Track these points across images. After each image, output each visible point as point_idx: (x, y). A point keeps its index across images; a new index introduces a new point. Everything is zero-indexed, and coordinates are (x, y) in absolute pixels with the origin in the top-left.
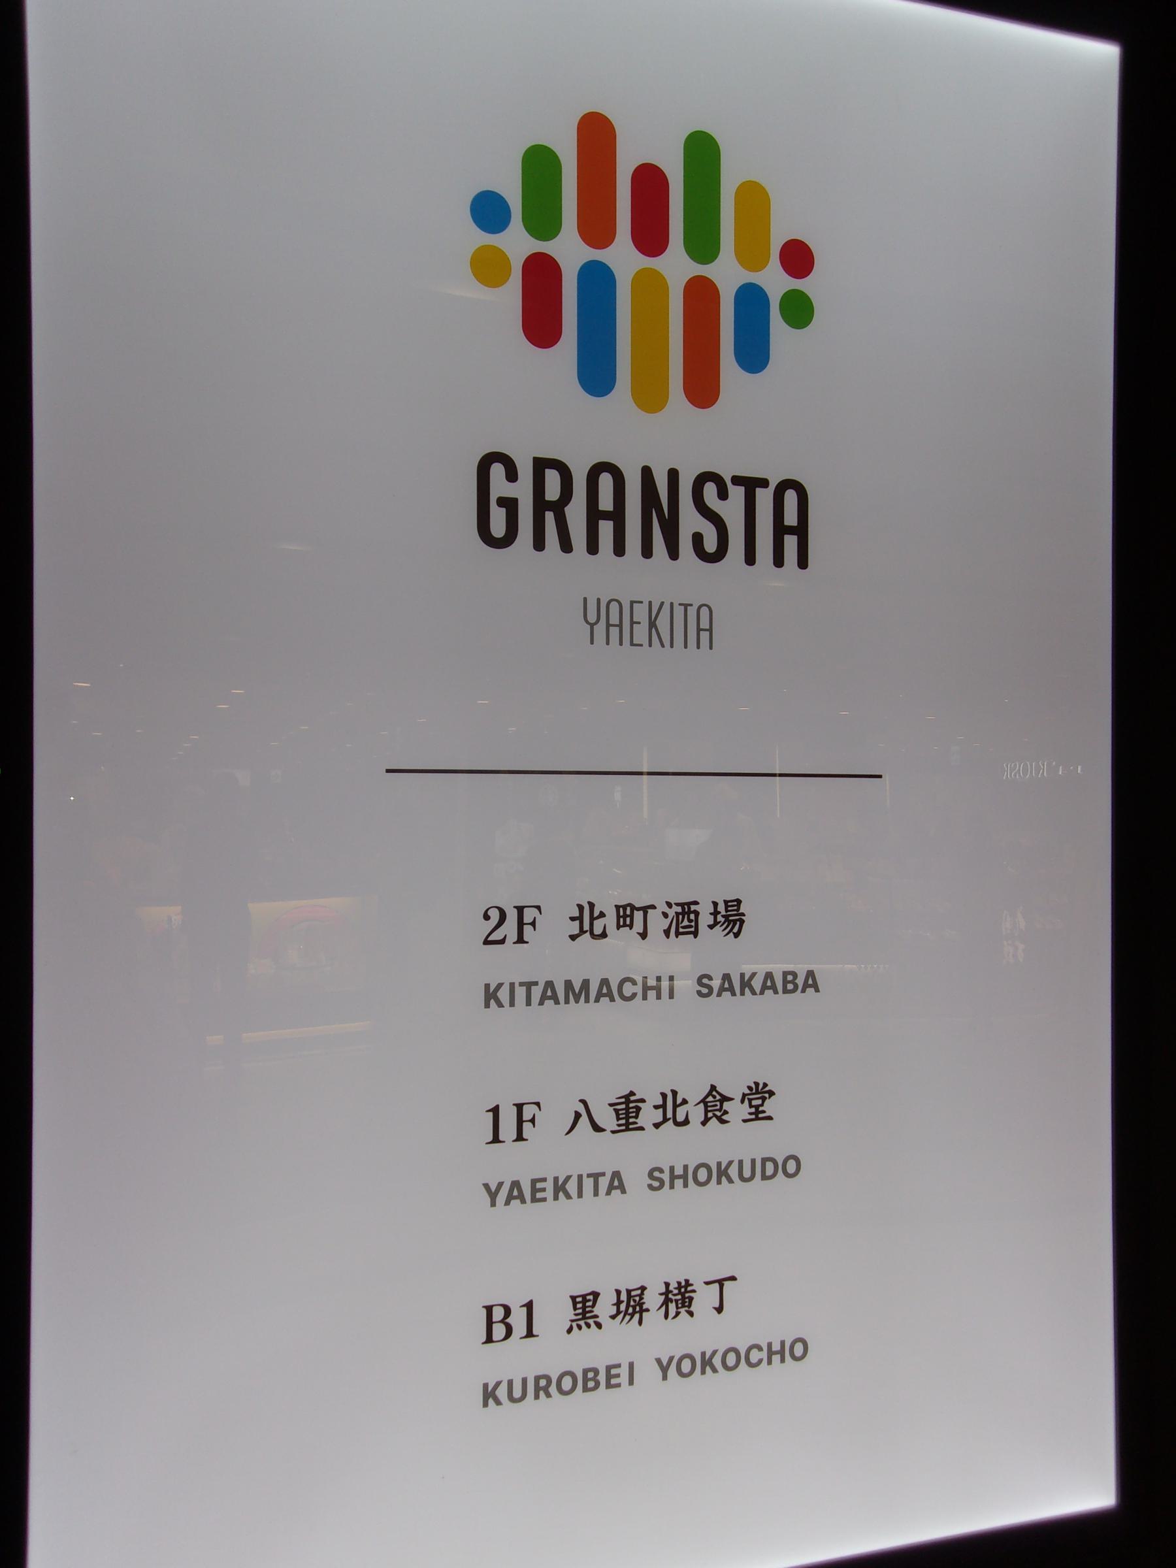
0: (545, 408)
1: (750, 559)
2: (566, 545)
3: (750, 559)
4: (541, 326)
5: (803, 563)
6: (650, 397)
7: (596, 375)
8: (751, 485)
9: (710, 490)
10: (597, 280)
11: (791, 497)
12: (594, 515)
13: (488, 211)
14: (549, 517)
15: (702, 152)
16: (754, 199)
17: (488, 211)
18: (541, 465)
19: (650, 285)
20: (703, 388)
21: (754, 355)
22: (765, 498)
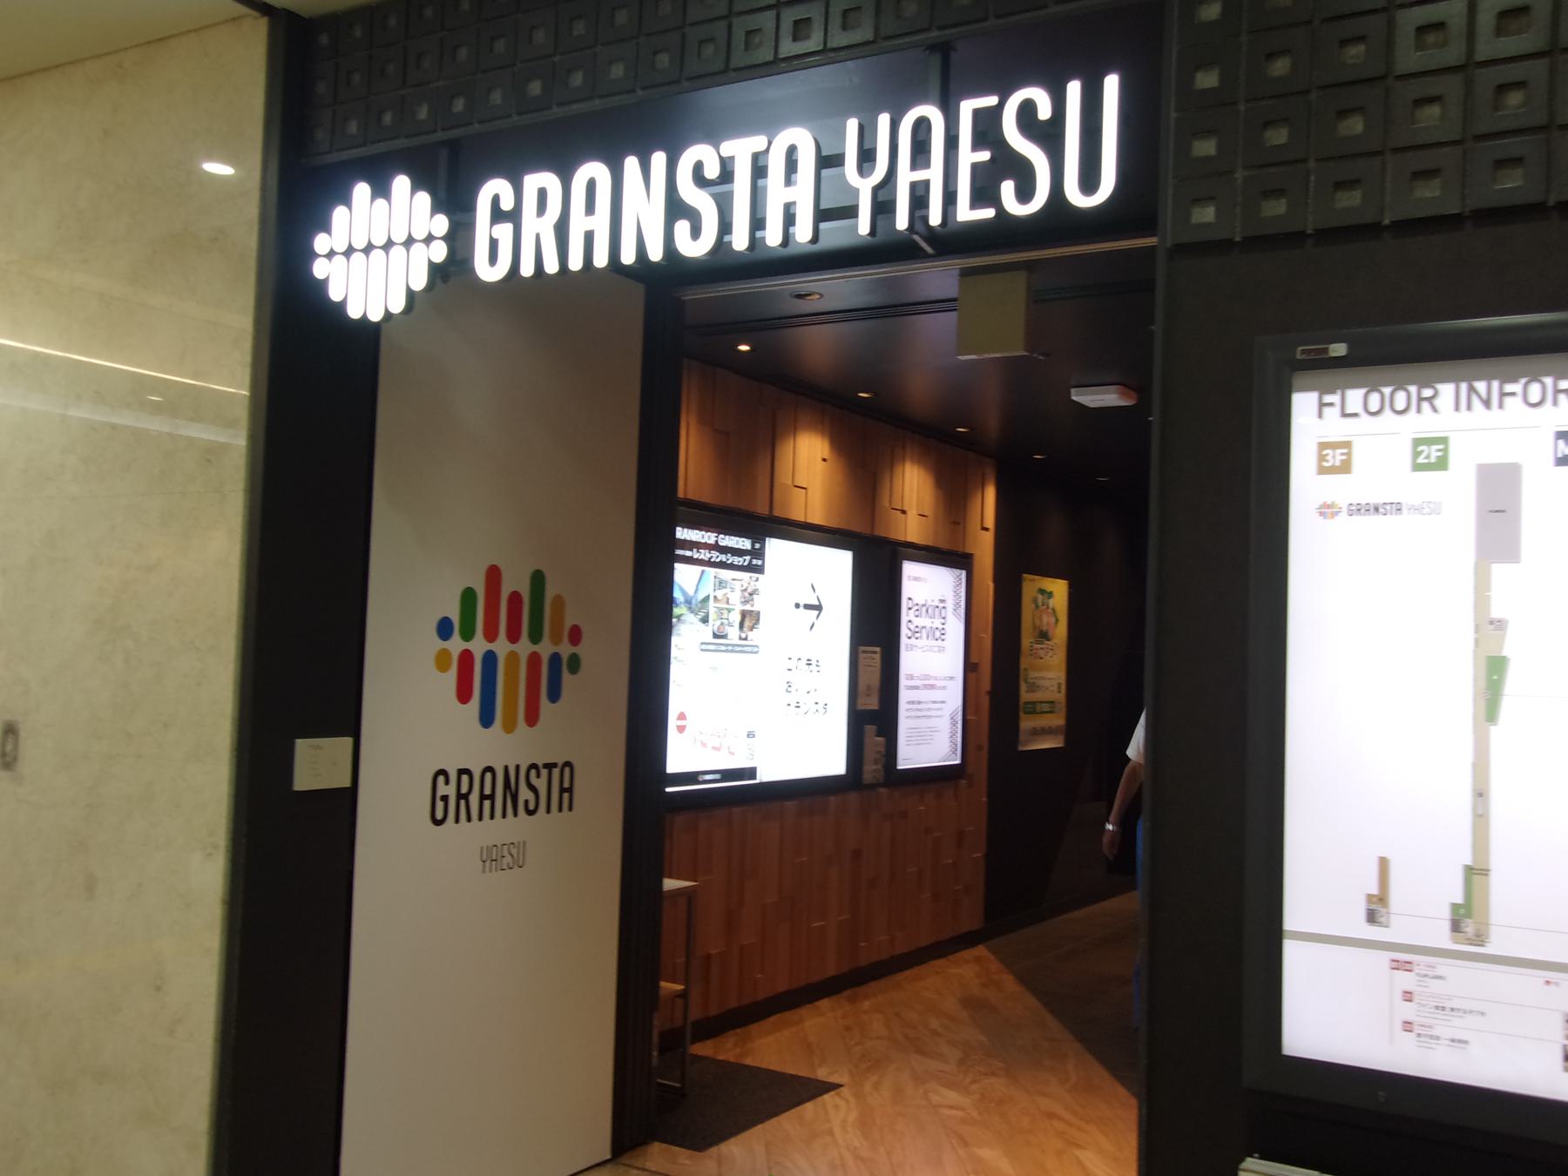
1: (548, 811)
2: (469, 819)
3: (548, 811)
4: (464, 695)
5: (570, 809)
6: (509, 727)
7: (486, 719)
8: (550, 766)
12: (483, 797)
14: (463, 802)
17: (444, 629)
18: (461, 772)
20: (532, 718)
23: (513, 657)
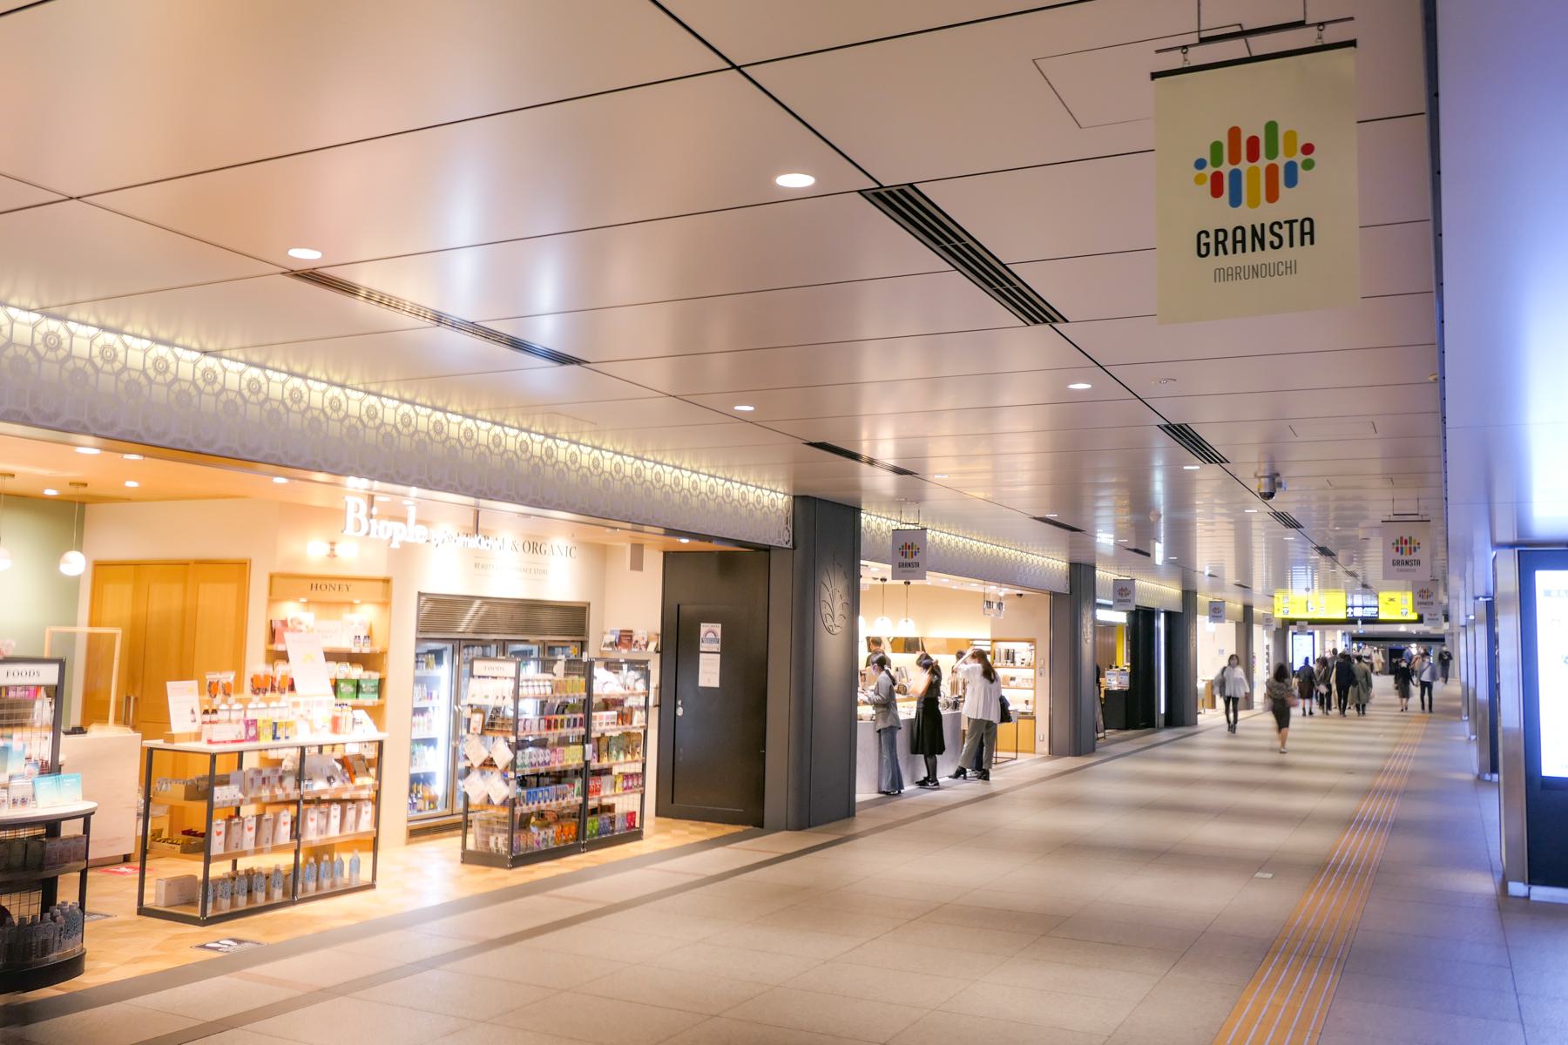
0: (1221, 214)
1: (1291, 245)
2: (1226, 253)
3: (1291, 245)
4: (1216, 191)
5: (1312, 242)
7: (1235, 201)
8: (1291, 223)
9: (1276, 228)
10: (1236, 176)
11: (1307, 224)
12: (1235, 242)
13: (1200, 164)
15: (1271, 128)
16: (1291, 135)
18: (1217, 231)
19: (1253, 173)
20: (1272, 196)
21: (1291, 181)
22: (1296, 226)
23: (1253, 173)
